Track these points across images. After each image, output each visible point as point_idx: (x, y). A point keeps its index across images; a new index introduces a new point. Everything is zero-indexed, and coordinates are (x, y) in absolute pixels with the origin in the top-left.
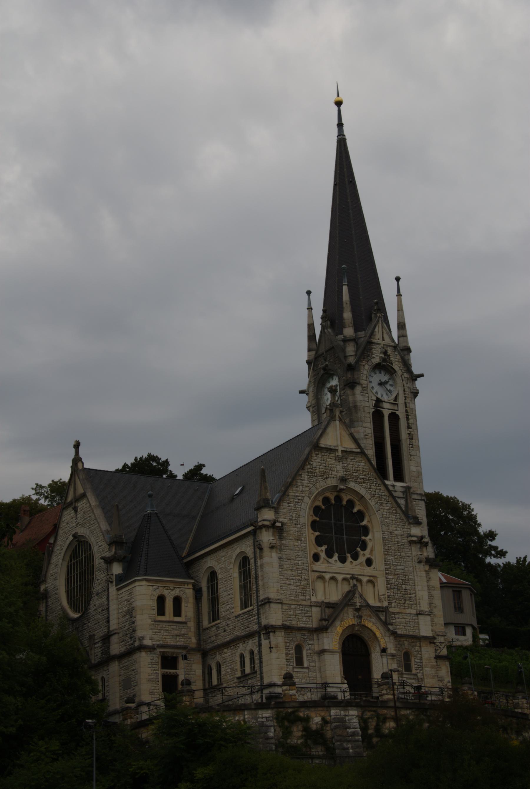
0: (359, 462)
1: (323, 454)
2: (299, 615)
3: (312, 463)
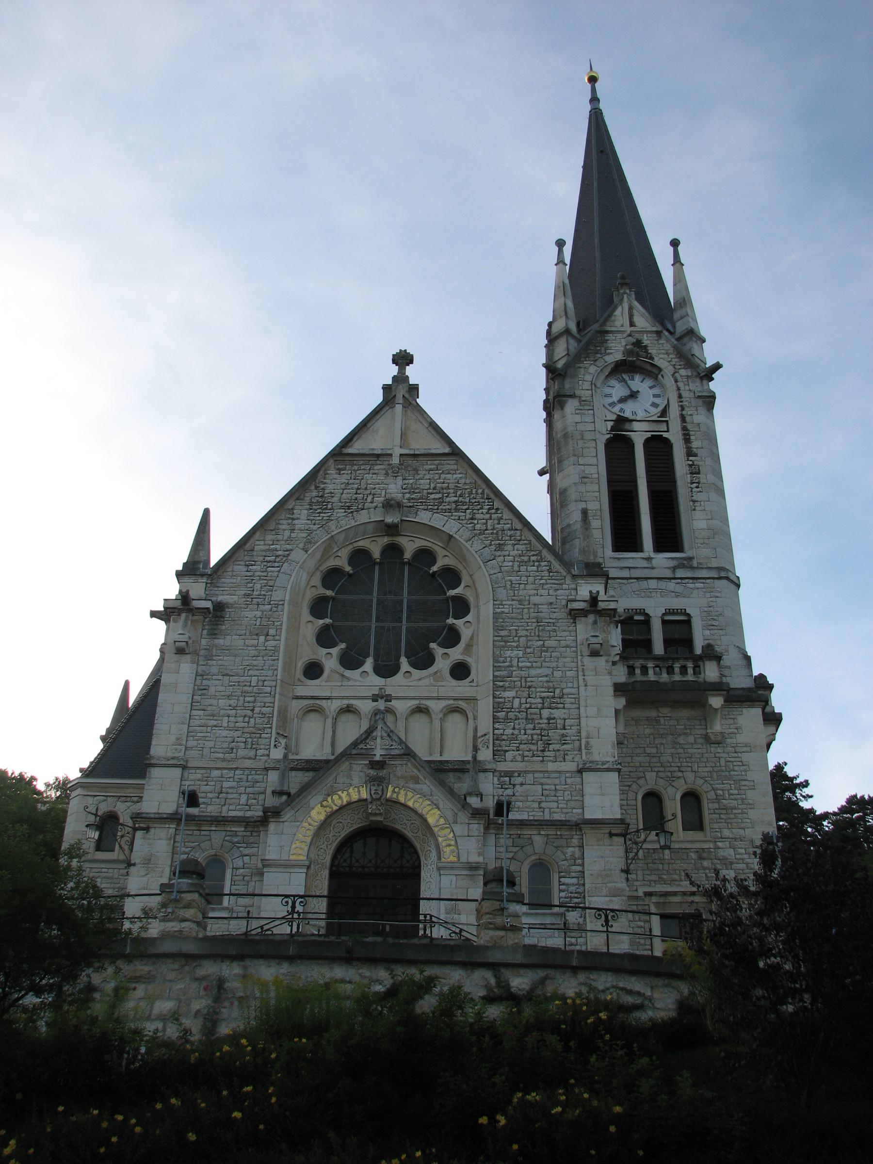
1: (356, 467)
2: (230, 791)
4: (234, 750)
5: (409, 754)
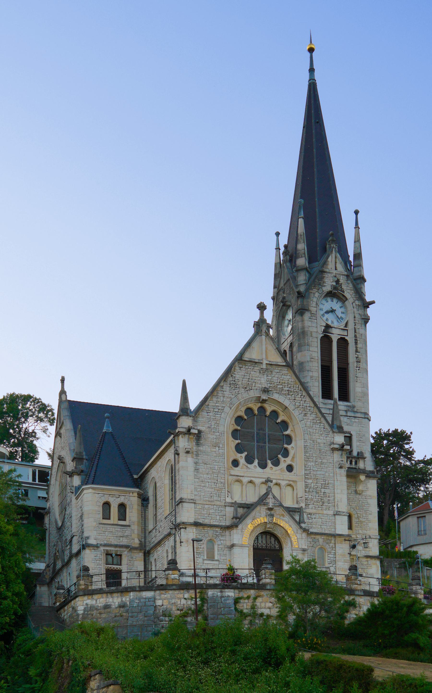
0: (285, 375)
1: (247, 367)
3: (234, 375)
5: (281, 505)
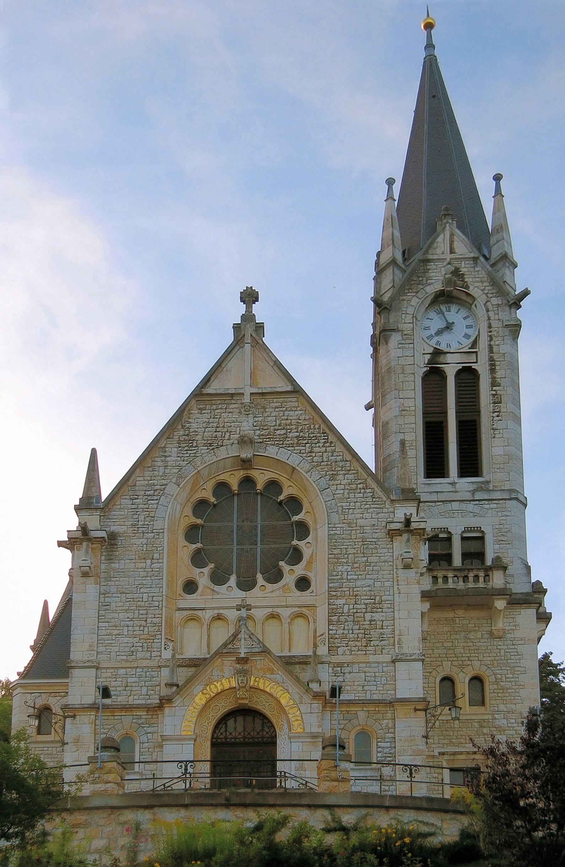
1: (214, 407)
2: (133, 684)
4: (134, 653)
5: (265, 651)
